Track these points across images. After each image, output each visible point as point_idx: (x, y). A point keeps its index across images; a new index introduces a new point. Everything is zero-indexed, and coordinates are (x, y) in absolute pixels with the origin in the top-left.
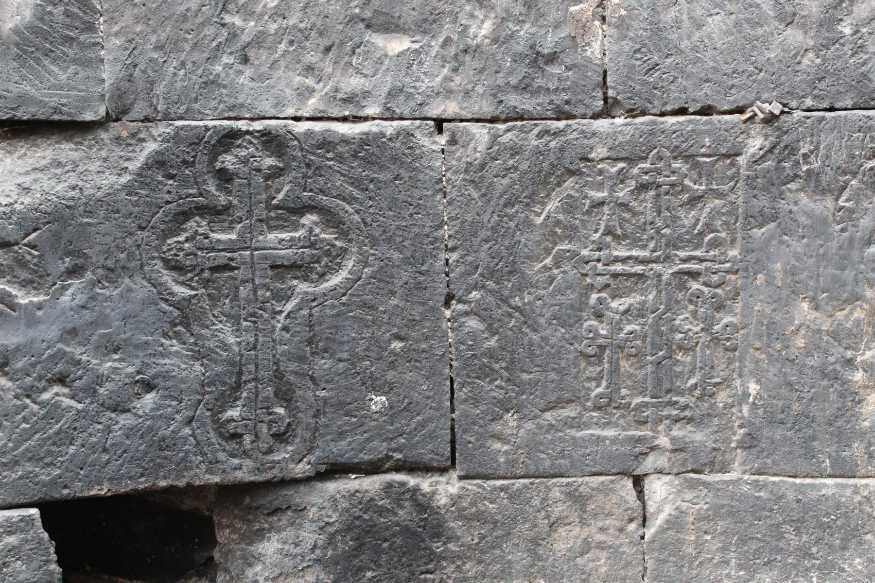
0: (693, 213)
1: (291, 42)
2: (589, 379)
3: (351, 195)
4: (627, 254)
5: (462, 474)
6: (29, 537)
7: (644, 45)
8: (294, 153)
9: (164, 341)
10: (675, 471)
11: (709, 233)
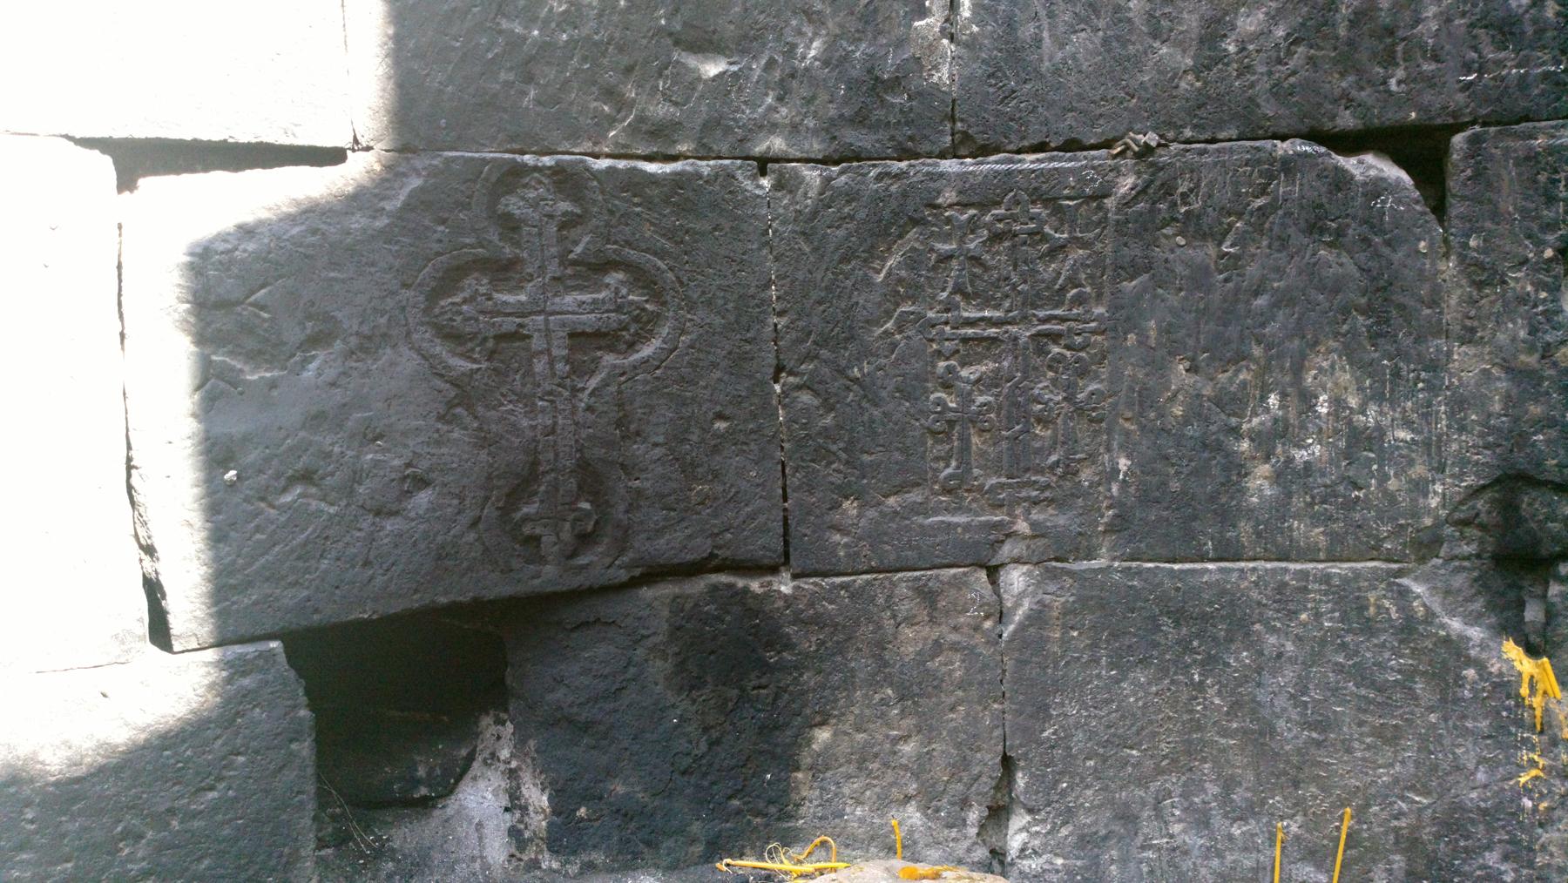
1: (585, 59)
2: (937, 459)
3: (663, 249)
5: (798, 571)
6: (270, 677)
7: (1000, 69)
10: (1035, 559)
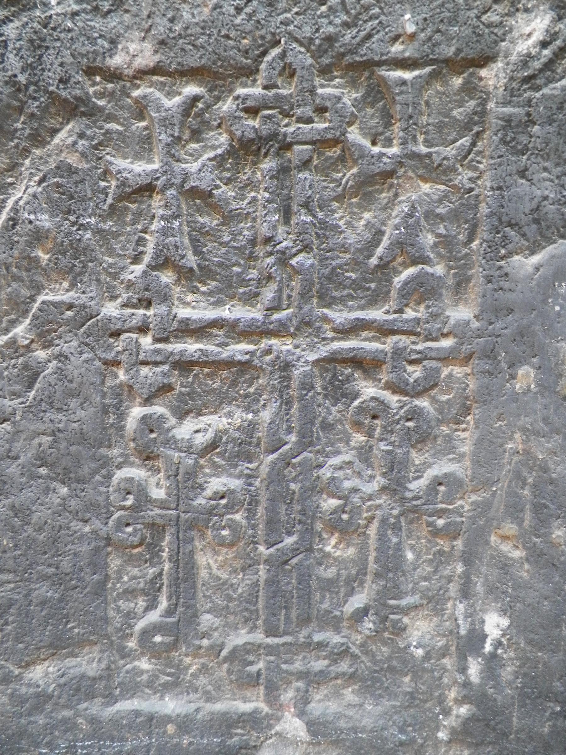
0: (367, 215)
2: (130, 593)
4: (211, 314)
11: (406, 265)
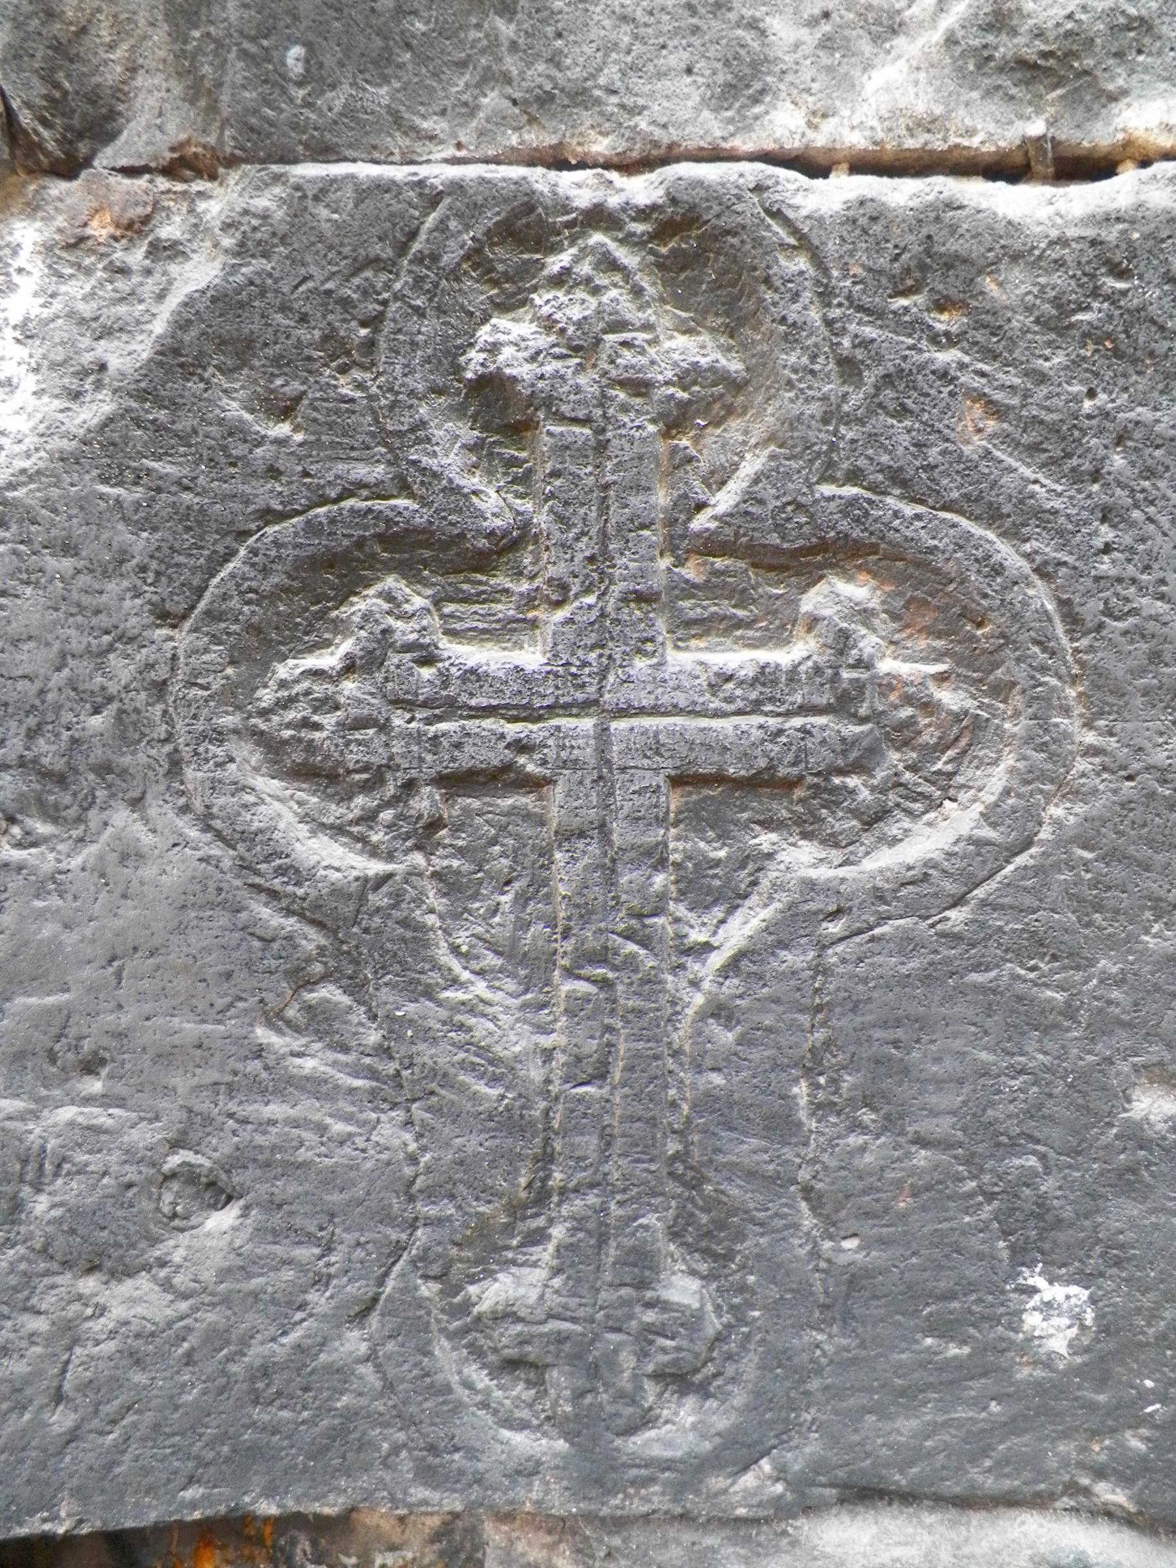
3: (1023, 499)
8: (793, 312)
9: (262, 1034)
